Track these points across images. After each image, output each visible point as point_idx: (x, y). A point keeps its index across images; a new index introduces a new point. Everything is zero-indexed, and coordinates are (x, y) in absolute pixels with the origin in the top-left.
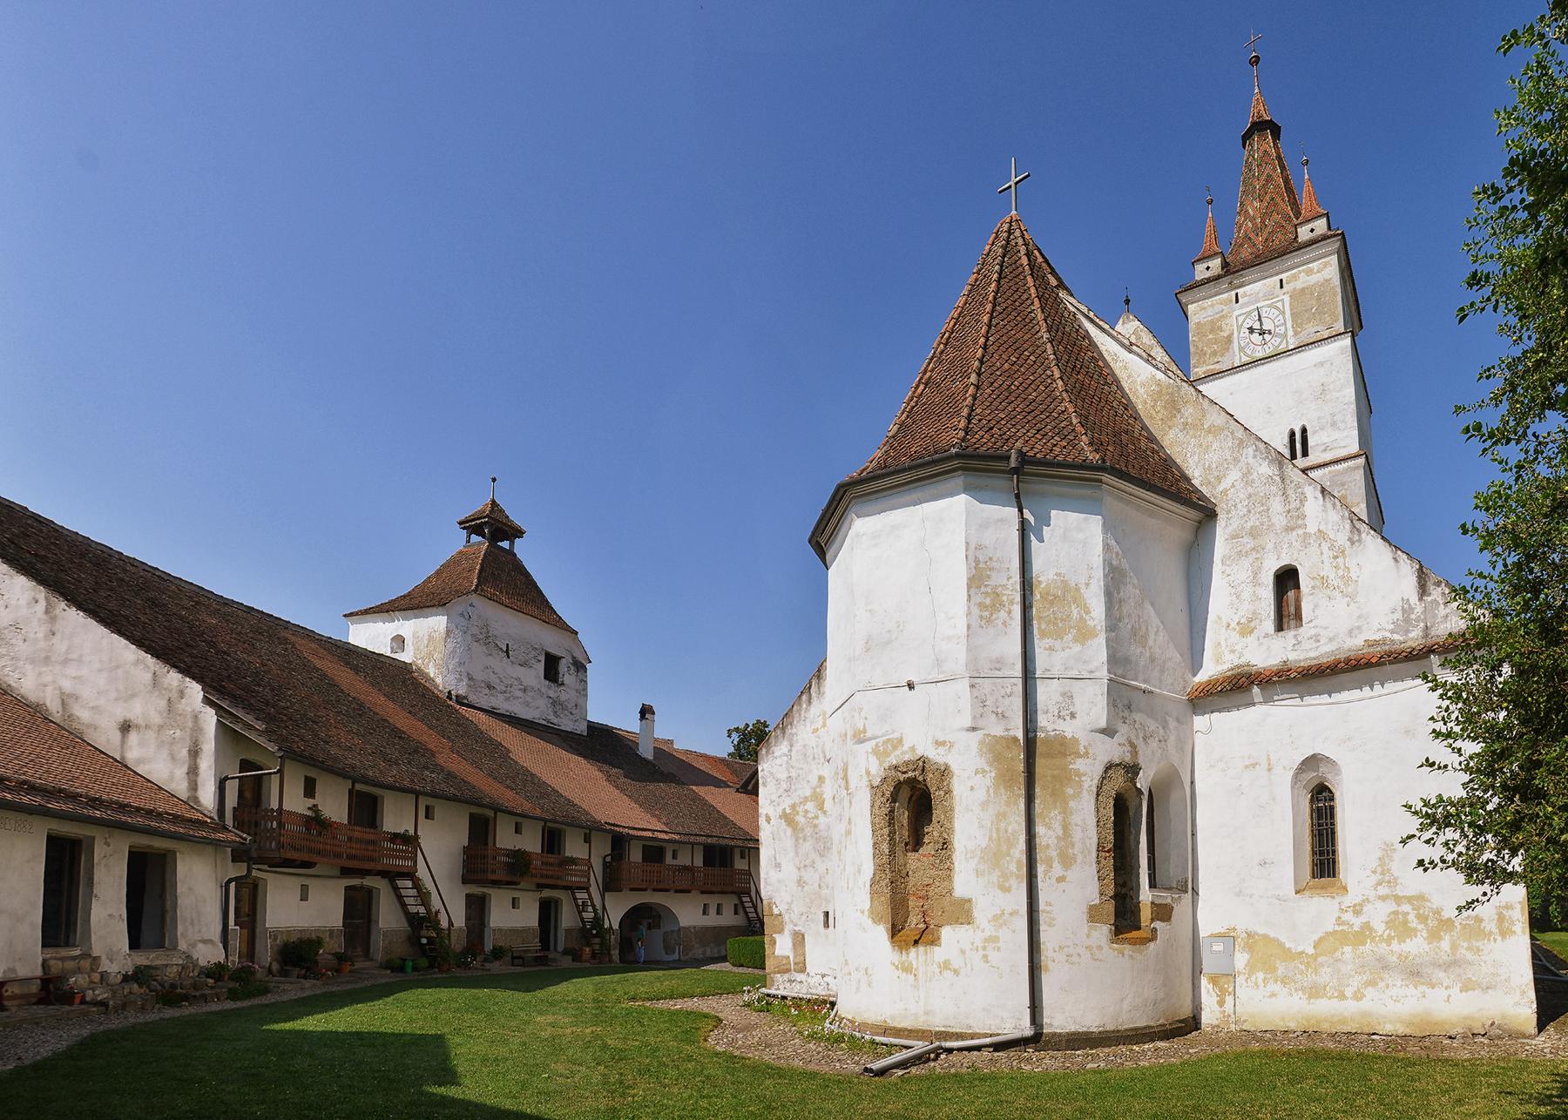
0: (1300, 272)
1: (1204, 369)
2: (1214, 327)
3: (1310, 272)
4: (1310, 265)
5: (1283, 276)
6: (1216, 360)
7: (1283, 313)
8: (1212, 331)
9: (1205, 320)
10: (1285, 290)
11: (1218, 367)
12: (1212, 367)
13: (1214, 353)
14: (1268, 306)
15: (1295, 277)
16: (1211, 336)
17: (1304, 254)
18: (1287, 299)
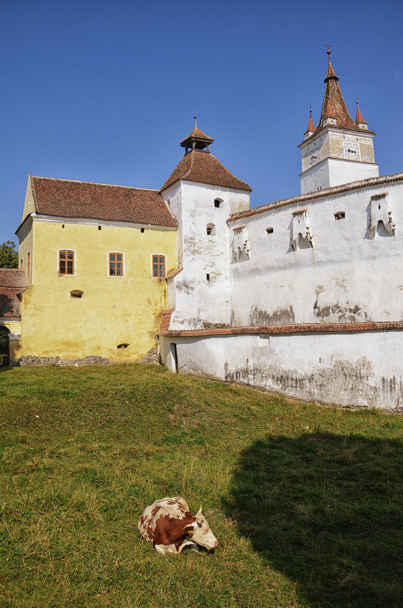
0: (362, 139)
1: (335, 155)
2: (338, 143)
3: (365, 140)
4: (365, 138)
5: (358, 137)
6: (338, 154)
7: (358, 149)
8: (337, 144)
9: (335, 139)
10: (359, 141)
11: (339, 157)
12: (338, 156)
13: (338, 152)
14: (354, 145)
15: (361, 139)
16: (336, 145)
17: (365, 134)
18: (359, 144)
